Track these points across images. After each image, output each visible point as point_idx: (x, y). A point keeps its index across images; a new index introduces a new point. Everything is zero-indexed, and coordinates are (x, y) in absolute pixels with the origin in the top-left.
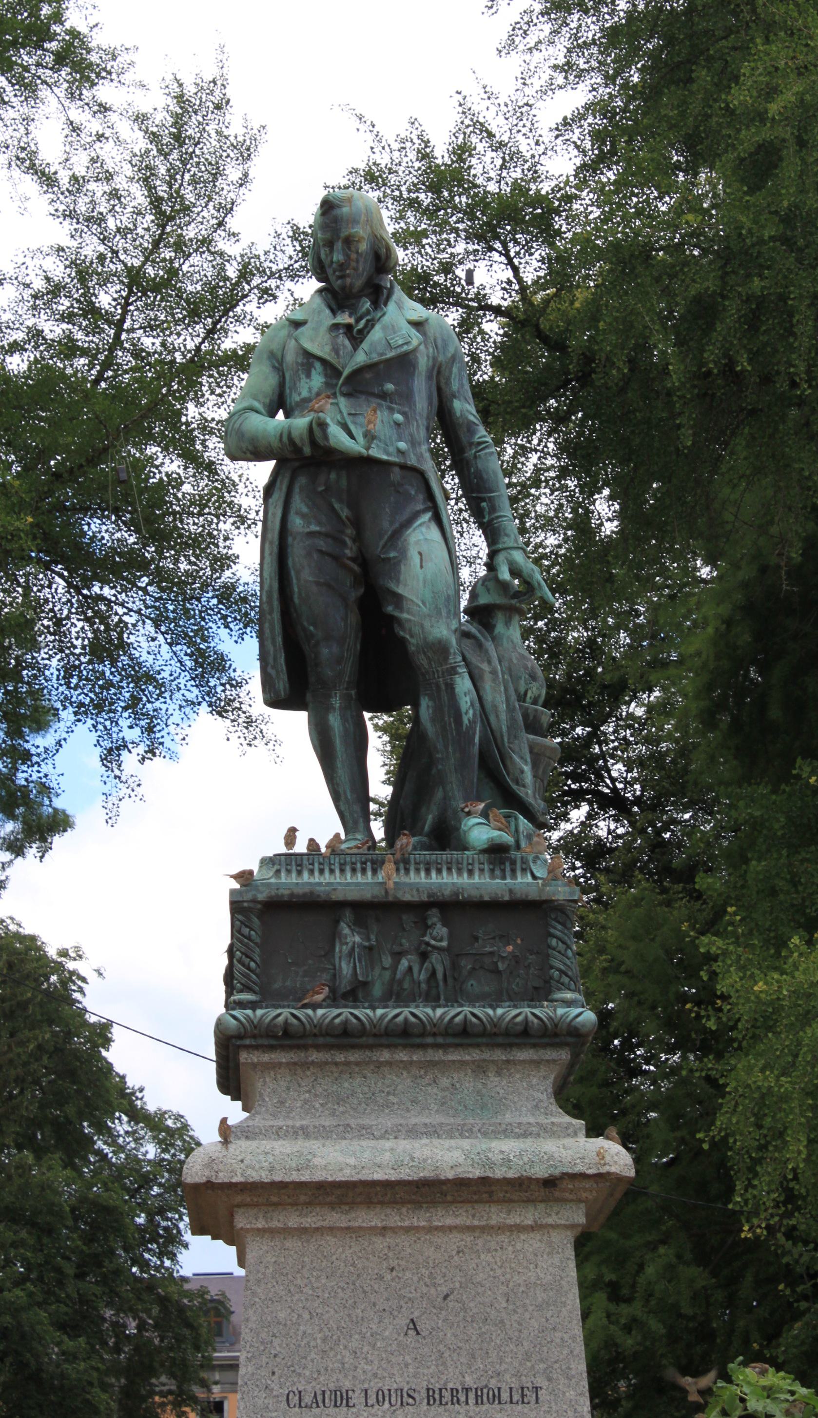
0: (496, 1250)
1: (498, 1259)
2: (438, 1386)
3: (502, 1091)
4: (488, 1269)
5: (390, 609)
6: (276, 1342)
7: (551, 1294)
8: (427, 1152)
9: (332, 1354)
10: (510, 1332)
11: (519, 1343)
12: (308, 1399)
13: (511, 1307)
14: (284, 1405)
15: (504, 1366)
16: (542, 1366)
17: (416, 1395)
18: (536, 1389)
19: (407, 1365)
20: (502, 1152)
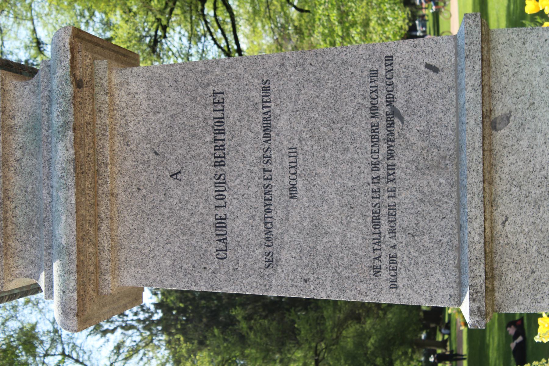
0: (126, 120)
1: (132, 119)
2: (213, 159)
3: (24, 116)
4: (138, 125)
6: (185, 266)
7: (154, 84)
8: (58, 167)
9: (193, 230)
10: (179, 111)
11: (185, 105)
12: (221, 246)
13: (162, 110)
14: (225, 261)
15: (200, 115)
16: (200, 90)
17: (219, 174)
18: (215, 93)
19: (200, 180)
20: (58, 116)
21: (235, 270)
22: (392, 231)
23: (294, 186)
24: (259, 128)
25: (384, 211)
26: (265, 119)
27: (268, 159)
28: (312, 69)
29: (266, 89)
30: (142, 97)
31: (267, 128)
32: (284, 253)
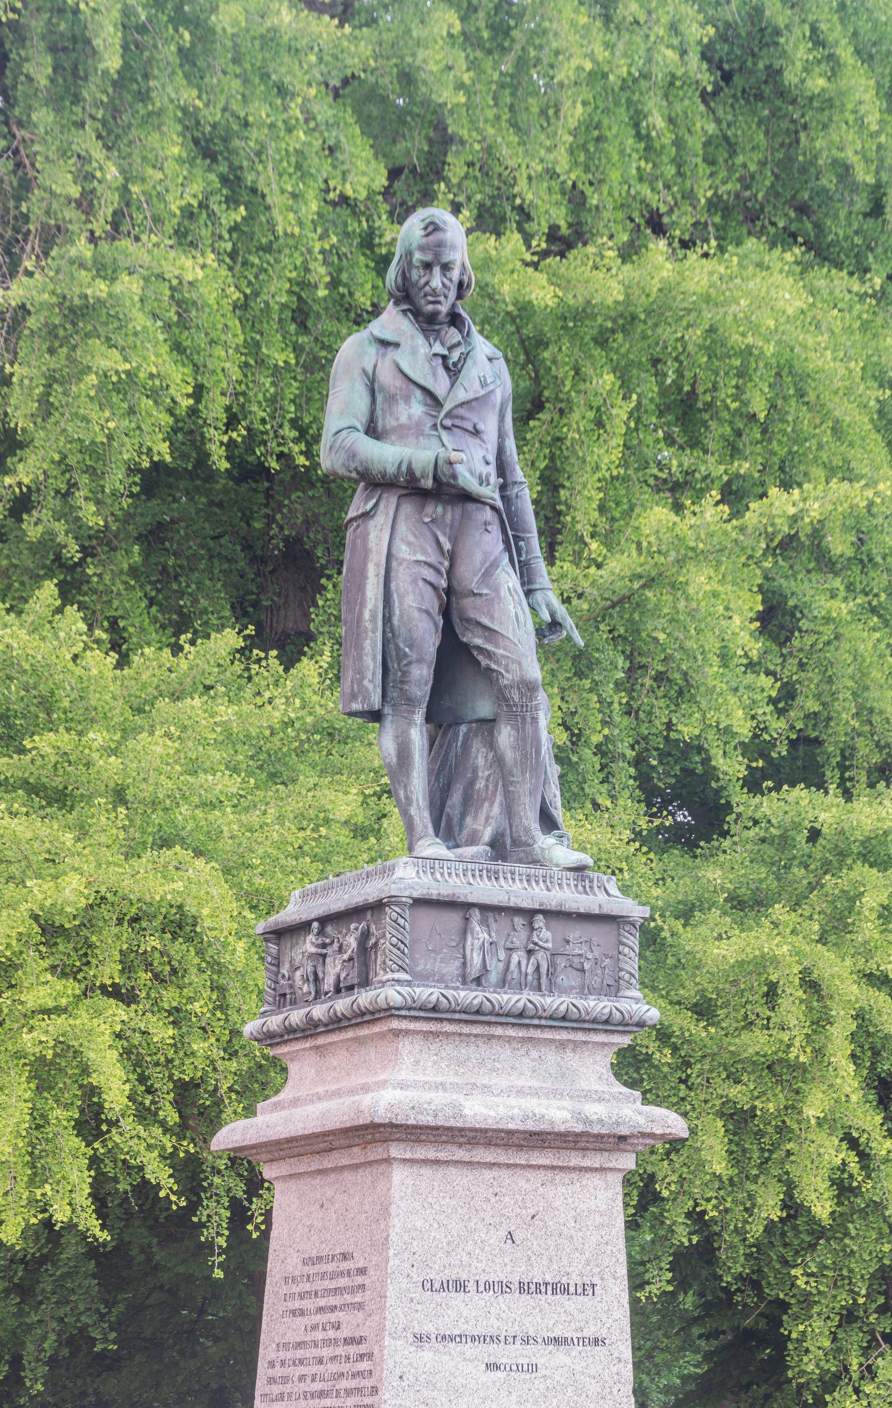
12: (437, 1285)
18: (593, 1285)
21: (412, 1300)
23: (498, 1368)
24: (557, 1333)
26: (566, 1339)
27: (526, 1341)
28: (615, 1391)
29: (596, 1341)
30: (593, 1204)
31: (557, 1341)
32: (431, 1354)
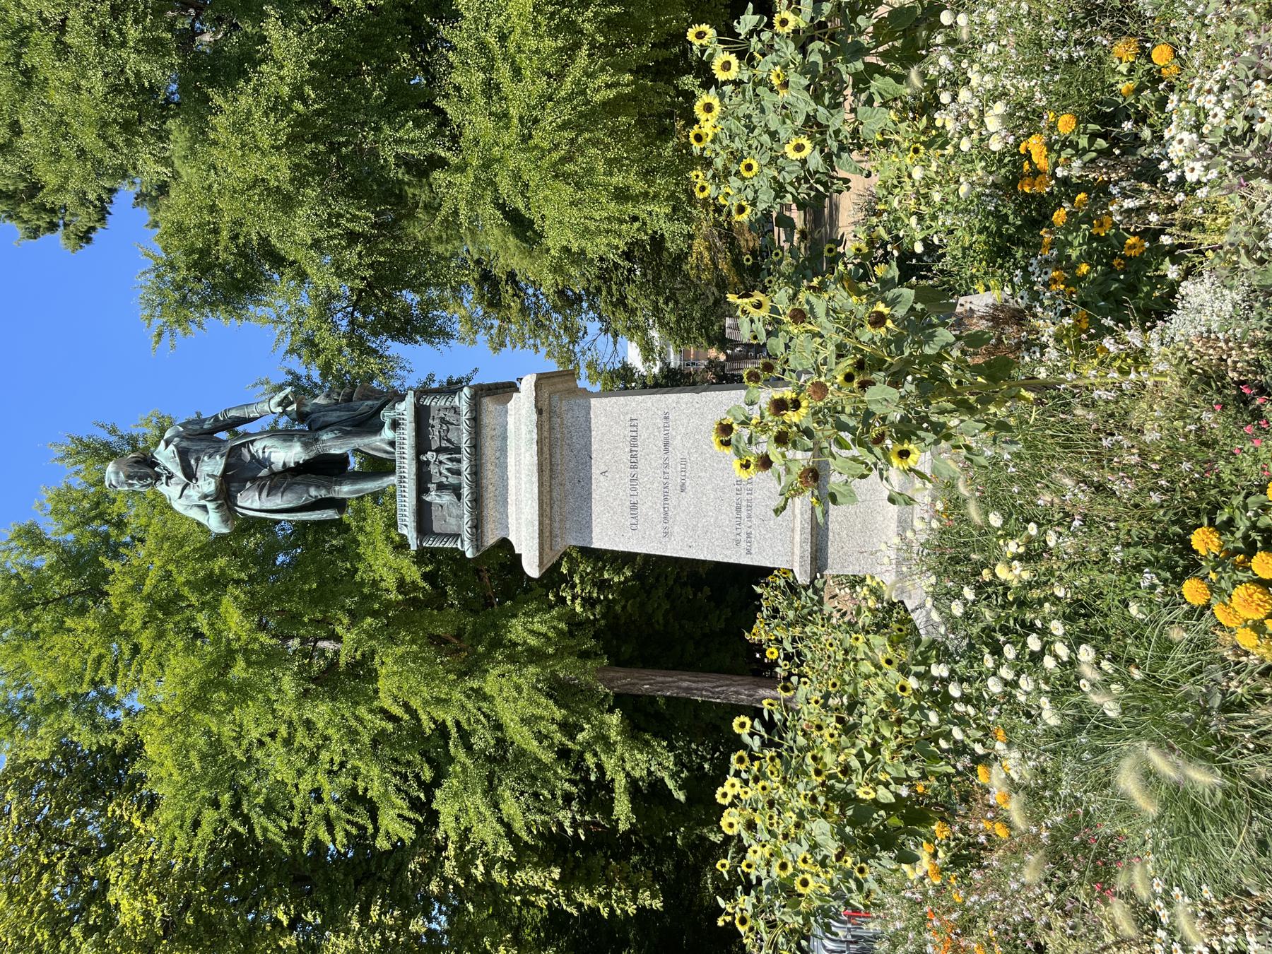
5: (292, 465)
22: (749, 517)
24: (661, 444)
25: (744, 503)
